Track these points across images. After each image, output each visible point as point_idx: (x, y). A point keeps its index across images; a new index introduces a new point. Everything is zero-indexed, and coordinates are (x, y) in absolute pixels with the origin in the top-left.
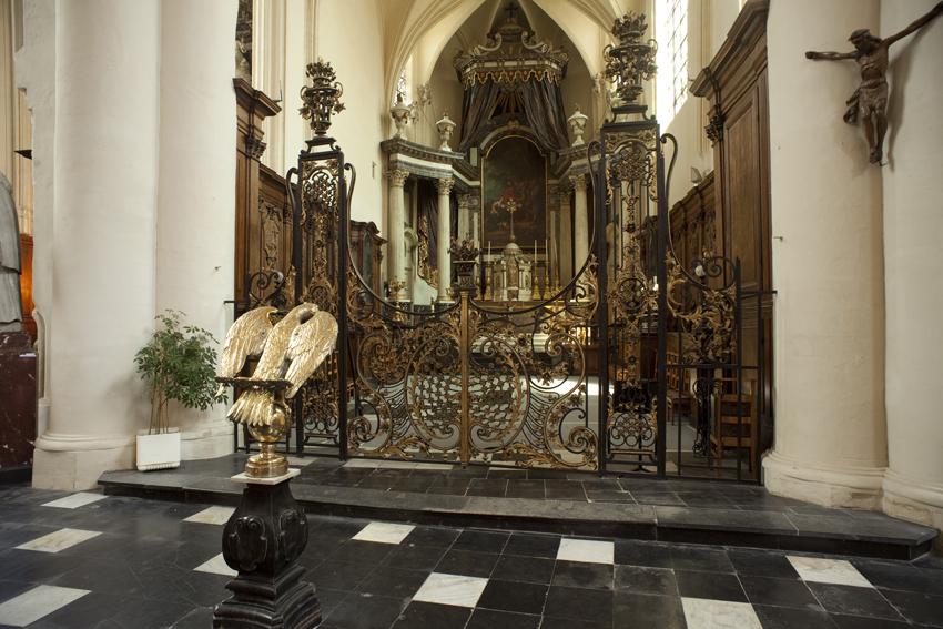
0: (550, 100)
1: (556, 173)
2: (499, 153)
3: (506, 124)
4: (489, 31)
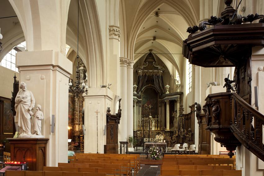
2: (146, 92)
3: (148, 84)
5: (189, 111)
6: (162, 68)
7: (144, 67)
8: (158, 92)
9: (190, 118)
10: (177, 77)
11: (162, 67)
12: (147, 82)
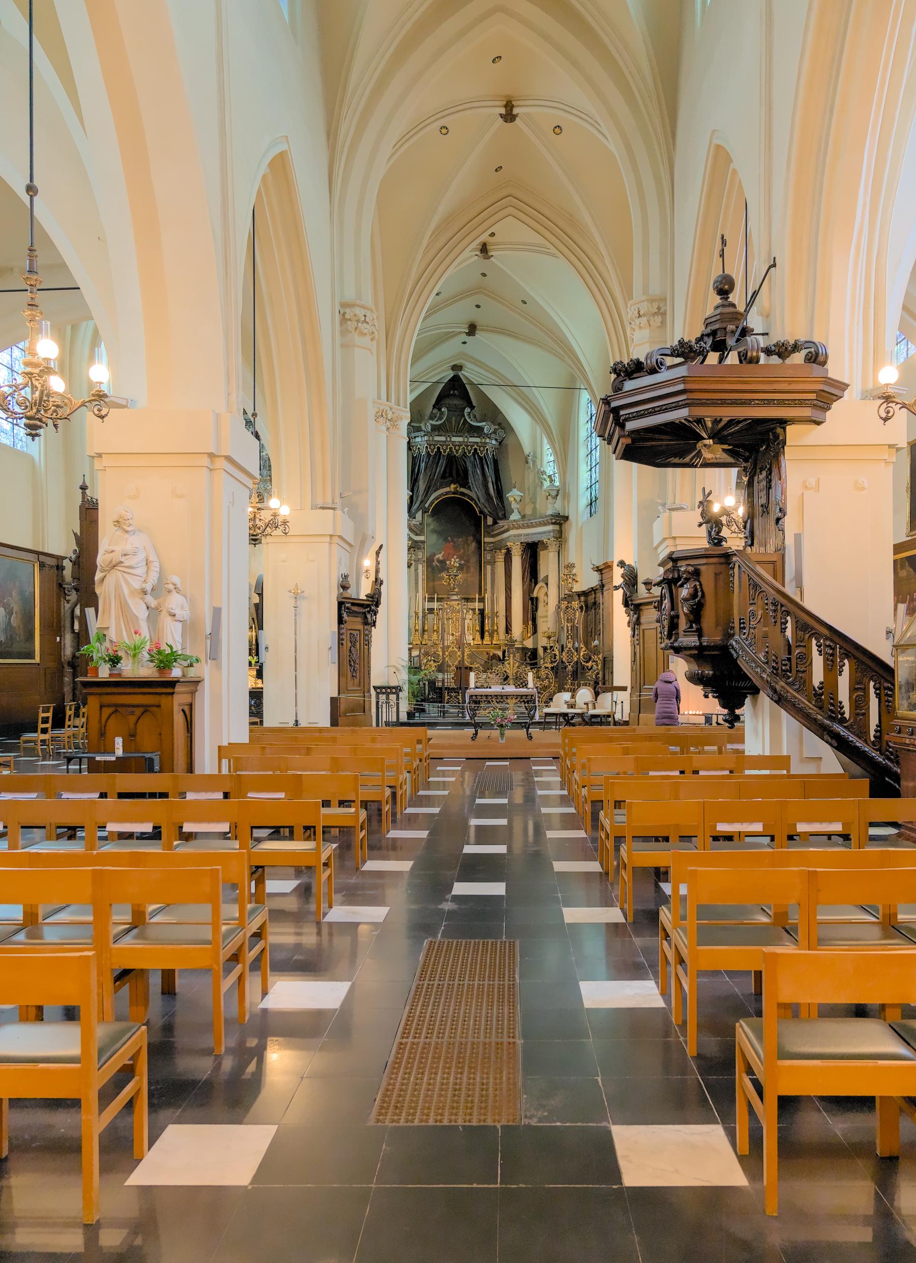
1: (492, 534)
4: (433, 404)
5: (587, 580)
6: (495, 432)
7: (431, 425)
8: (481, 512)
9: (595, 603)
10: (548, 463)
11: (497, 427)
12: (443, 476)
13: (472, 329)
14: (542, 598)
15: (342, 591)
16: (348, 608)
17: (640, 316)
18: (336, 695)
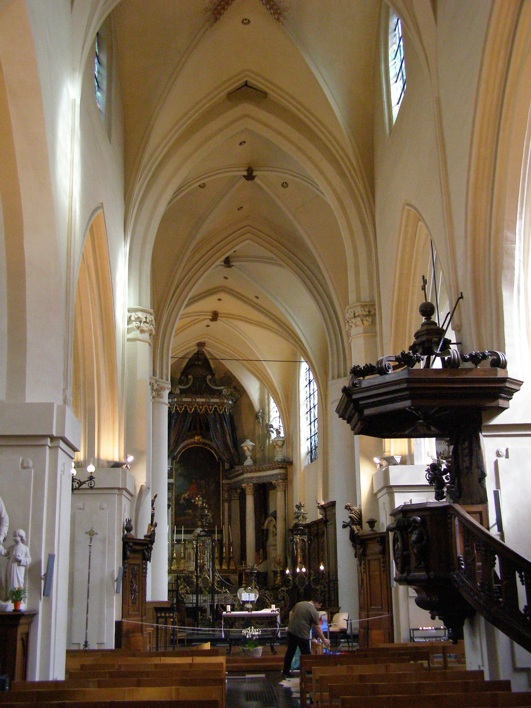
0: (227, 427)
3: (192, 437)
6: (231, 394)
7: (180, 389)
8: (220, 459)
12: (189, 430)
13: (215, 316)
14: (271, 528)
15: (126, 532)
16: (131, 547)
17: (355, 317)
18: (120, 619)
